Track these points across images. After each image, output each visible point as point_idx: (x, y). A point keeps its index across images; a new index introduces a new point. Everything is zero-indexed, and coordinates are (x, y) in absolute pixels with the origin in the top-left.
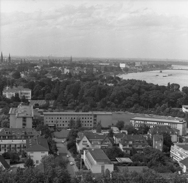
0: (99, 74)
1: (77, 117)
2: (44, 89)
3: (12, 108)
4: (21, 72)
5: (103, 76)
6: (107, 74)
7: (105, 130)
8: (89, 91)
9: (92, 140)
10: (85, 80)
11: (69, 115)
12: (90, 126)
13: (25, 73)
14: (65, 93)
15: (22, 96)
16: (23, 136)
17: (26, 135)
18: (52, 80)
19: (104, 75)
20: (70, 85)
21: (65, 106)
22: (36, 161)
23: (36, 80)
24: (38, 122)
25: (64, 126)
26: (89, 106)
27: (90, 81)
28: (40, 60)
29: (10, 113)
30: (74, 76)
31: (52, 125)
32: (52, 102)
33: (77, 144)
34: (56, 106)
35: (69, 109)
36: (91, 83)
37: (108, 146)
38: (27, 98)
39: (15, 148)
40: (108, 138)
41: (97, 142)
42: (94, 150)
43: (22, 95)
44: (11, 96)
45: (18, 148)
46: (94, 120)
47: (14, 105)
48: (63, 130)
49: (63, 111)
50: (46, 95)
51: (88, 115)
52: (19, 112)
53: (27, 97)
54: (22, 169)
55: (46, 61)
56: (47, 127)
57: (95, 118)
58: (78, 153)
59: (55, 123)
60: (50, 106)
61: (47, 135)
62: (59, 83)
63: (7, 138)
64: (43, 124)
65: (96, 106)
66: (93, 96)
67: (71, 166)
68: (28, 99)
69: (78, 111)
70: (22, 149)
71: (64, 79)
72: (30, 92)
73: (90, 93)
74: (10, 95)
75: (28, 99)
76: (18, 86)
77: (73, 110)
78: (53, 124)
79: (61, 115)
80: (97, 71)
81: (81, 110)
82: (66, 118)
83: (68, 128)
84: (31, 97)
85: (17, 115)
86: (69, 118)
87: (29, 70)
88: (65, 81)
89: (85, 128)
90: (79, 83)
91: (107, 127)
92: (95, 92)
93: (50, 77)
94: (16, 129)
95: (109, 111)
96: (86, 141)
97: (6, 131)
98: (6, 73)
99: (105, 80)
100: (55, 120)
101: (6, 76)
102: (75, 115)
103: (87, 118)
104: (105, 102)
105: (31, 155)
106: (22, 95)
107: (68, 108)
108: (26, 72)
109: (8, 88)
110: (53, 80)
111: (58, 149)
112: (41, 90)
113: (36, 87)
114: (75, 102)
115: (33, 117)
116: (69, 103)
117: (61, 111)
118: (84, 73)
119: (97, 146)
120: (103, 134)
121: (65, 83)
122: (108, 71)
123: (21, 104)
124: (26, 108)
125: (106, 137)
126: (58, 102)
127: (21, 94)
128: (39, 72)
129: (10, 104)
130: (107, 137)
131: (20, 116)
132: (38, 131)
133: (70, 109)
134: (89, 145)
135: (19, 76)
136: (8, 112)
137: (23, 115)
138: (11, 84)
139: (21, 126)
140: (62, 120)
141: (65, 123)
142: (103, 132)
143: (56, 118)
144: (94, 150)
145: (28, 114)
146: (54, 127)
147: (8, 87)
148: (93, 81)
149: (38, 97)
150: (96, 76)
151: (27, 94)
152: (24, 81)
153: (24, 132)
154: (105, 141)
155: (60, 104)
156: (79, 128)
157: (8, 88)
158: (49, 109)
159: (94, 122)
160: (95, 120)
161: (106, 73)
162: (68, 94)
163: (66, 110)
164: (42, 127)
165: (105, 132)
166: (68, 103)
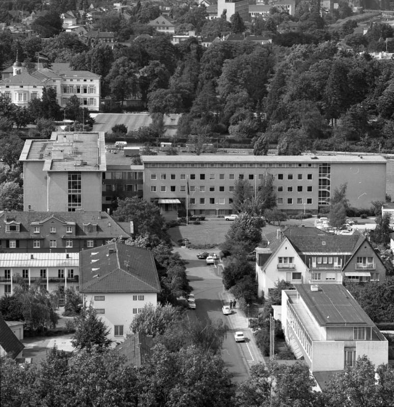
0: (343, 18)
1: (262, 171)
2: (146, 75)
3: (30, 141)
4: (64, 11)
5: (354, 24)
6: (372, 17)
7: (359, 220)
8: (304, 79)
9: (312, 254)
10: (287, 41)
11: (232, 164)
12: (305, 206)
13: (79, 14)
14: (219, 89)
15: (69, 97)
16: (71, 239)
17: (81, 237)
18: (174, 42)
19: (360, 20)
20: (236, 59)
21: (219, 134)
22: (116, 327)
23: (119, 40)
24: (124, 189)
25: (213, 203)
26: (301, 132)
27: (306, 45)
29: (23, 158)
30: (252, 26)
31: (171, 201)
32: (172, 120)
33: (258, 268)
34: (188, 131)
35: (233, 145)
36: (311, 52)
37: (369, 274)
38: (86, 106)
39: (42, 282)
40: (369, 247)
41: (331, 263)
42: (316, 289)
43: (69, 95)
44: (29, 99)
45: (52, 281)
46: (320, 184)
47: (40, 128)
48: (211, 219)
49: (211, 152)
50: (151, 95)
51: (300, 165)
52: (55, 156)
53: (85, 103)
54: (65, 355)
56: (153, 209)
57: (324, 175)
58: (261, 301)
59: (185, 195)
60: (166, 134)
61: (154, 237)
62: (197, 53)
63: (13, 245)
64: (141, 197)
65: (330, 135)
66: (320, 98)
67: (238, 344)
68: (89, 109)
69: (262, 150)
70: (66, 286)
71: (216, 36)
72: (96, 83)
73: (308, 86)
74: (26, 93)
75: (90, 107)
76: (52, 64)
77: (246, 147)
78: (175, 199)
79: (202, 164)
80: (336, 6)
81: (273, 146)
82: (222, 176)
83: (230, 212)
84: (100, 101)
85: (47, 167)
86: (232, 176)
87: (92, 6)
88: (220, 43)
89: (289, 212)
90: (269, 50)
91: (368, 206)
92: (325, 84)
93: (166, 31)
94: (44, 215)
95: (374, 151)
96: (291, 259)
97: (8, 220)
98: (11, 17)
99: (363, 41)
100: (183, 182)
101: (11, 28)
102: (251, 164)
103: (295, 177)
104: (360, 120)
105: (97, 305)
106: (65, 94)
107: (231, 141)
108: (82, 12)
109: (18, 69)
110: (178, 40)
111: (191, 284)
112: (135, 77)
113: (117, 66)
114: (252, 117)
115: (104, 173)
116: (234, 124)
117: (204, 152)
118: (288, 14)
119: (331, 275)
120: (351, 234)
121: (220, 51)
122: (376, 7)
123: (63, 127)
124: (82, 142)
125: (363, 242)
126: (196, 120)
127: (65, 89)
128: (129, 12)
129: (25, 126)
130: (366, 244)
131: (59, 167)
132: (120, 223)
133: (238, 145)
134: (300, 273)
135: (57, 26)
136: (18, 156)
137: (70, 166)
138: (29, 55)
139: (63, 204)
140: (207, 183)
141: (216, 194)
142: (351, 224)
143: (188, 176)
144: (320, 290)
145: (88, 163)
146: (181, 209)
147: (19, 65)
148: (316, 43)
149: (125, 103)
150: (334, 25)
151: (85, 91)
152: (73, 44)
153: (72, 225)
154: (360, 259)
155: (202, 124)
156: (267, 210)
157: (18, 69)
158: (163, 144)
159: (322, 190)
160: (324, 182)
161: (368, 13)
162: (231, 90)
163: (221, 147)
164: (137, 208)
165: (359, 224)
166: (231, 122)
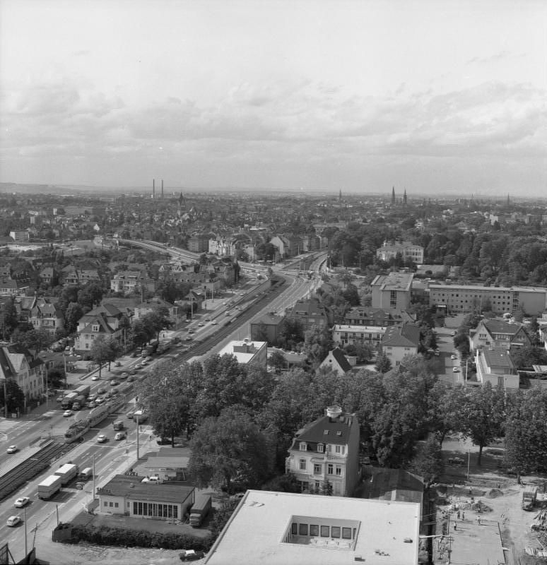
4: (418, 218)
28: (457, 200)
33: (470, 339)
39: (369, 339)
55: (465, 202)
65: (527, 279)
69: (488, 285)
72: (422, 251)
103: (502, 297)
114: (492, 270)
127: (407, 254)
135: (412, 224)
138: (393, 237)
140: (460, 298)
144: (493, 350)
152: (418, 234)
160: (515, 301)
